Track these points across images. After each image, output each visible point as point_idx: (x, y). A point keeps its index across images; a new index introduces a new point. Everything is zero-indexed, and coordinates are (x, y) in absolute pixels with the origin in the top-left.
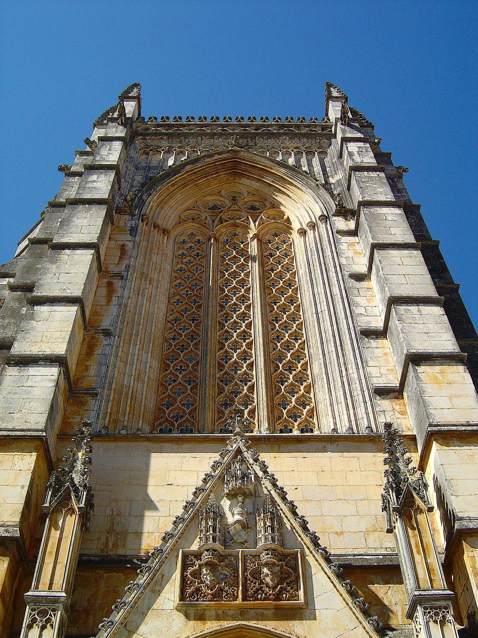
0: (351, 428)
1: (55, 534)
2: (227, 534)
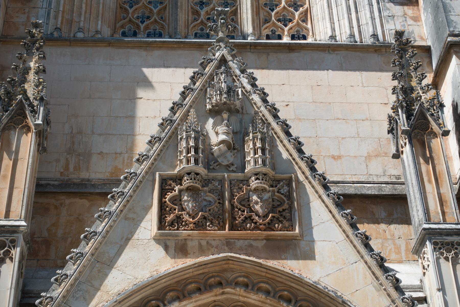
0: (352, 35)
2: (211, 157)
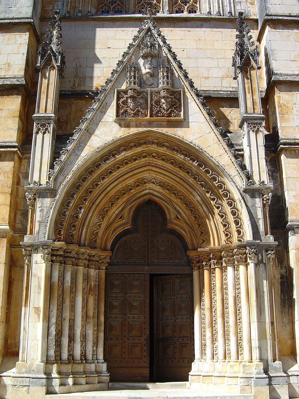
1: (45, 81)
